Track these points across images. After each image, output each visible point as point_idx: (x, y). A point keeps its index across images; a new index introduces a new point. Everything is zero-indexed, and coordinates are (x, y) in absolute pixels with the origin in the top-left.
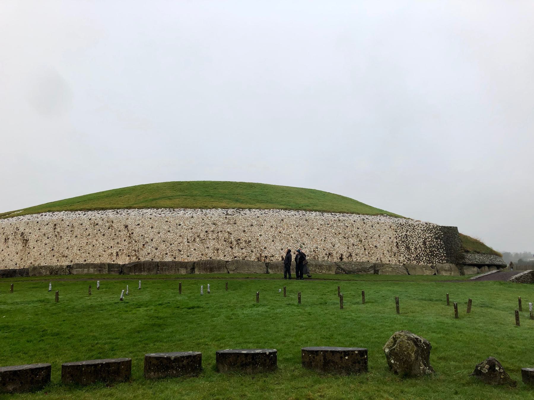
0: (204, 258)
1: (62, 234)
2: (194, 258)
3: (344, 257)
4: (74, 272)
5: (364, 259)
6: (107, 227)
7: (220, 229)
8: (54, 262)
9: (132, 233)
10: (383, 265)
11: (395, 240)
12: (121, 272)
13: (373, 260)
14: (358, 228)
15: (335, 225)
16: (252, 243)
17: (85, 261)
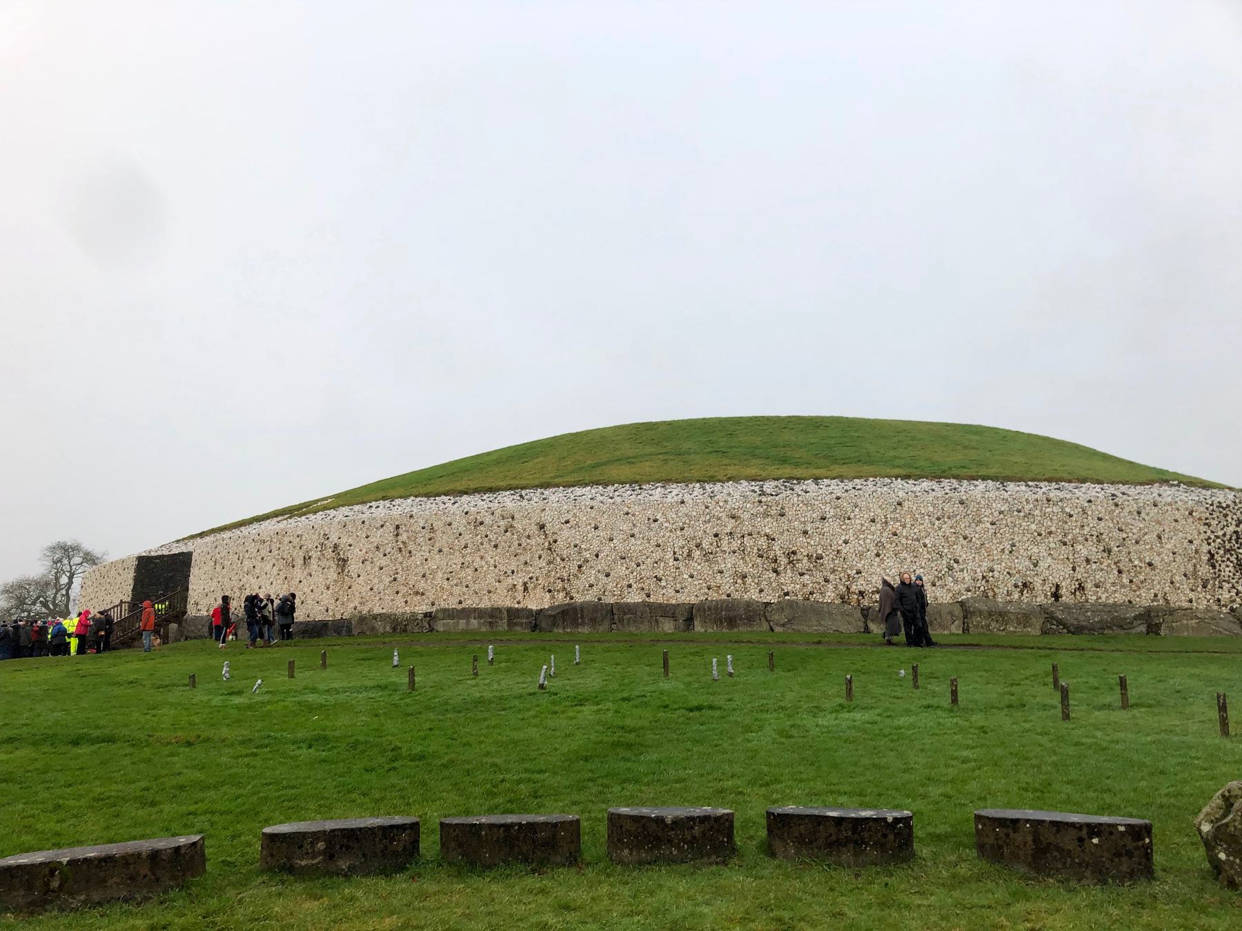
0: (713, 596)
1: (411, 546)
2: (691, 595)
3: (1063, 591)
4: (440, 626)
5: (1119, 597)
6: (502, 529)
7: (746, 528)
8: (398, 606)
9: (555, 541)
10: (1172, 612)
11: (1205, 548)
12: (535, 627)
13: (1144, 599)
14: (1100, 519)
15: (1037, 512)
16: (825, 561)
17: (460, 602)
